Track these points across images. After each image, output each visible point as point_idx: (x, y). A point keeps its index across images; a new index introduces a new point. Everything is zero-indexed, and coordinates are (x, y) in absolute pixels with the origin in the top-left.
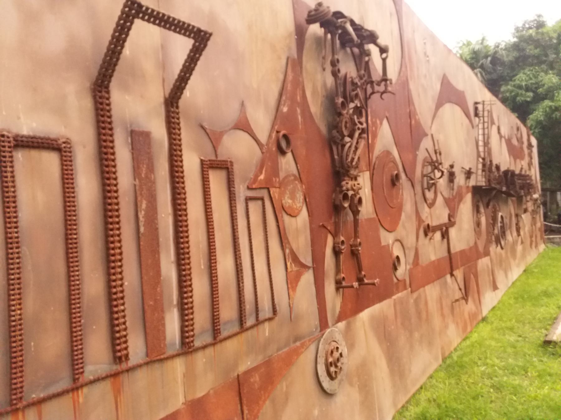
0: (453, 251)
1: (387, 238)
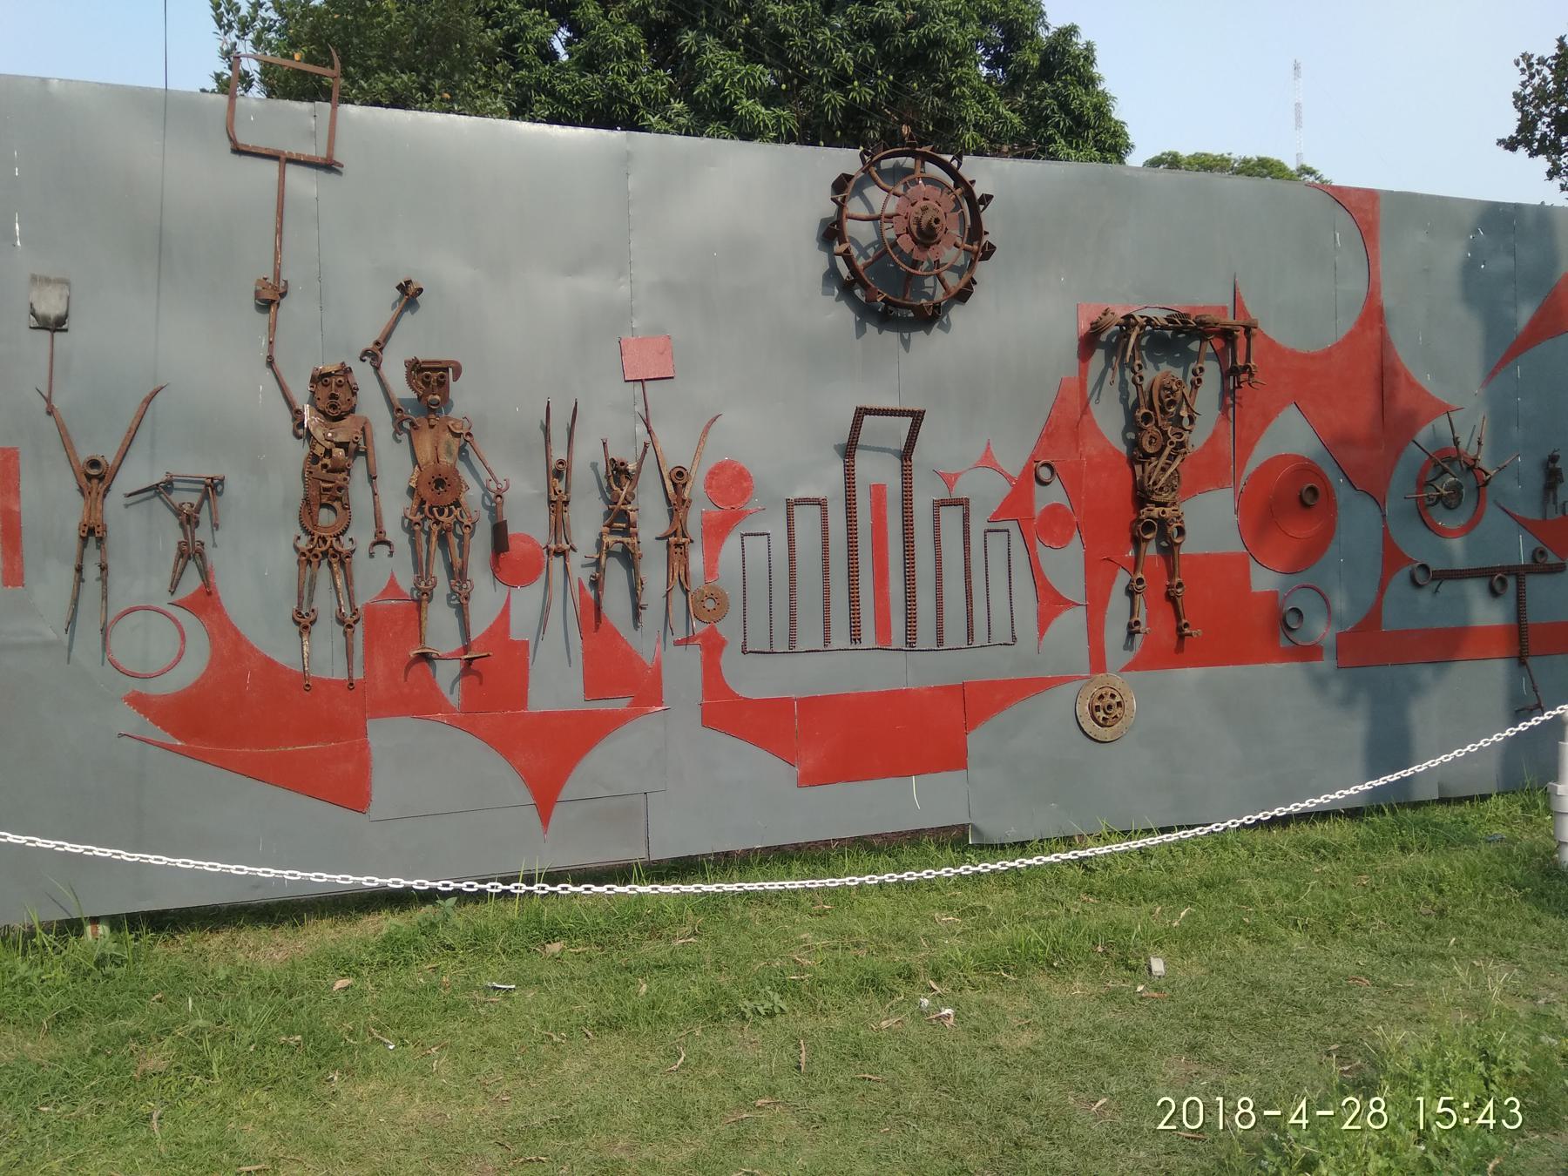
0: (1532, 618)
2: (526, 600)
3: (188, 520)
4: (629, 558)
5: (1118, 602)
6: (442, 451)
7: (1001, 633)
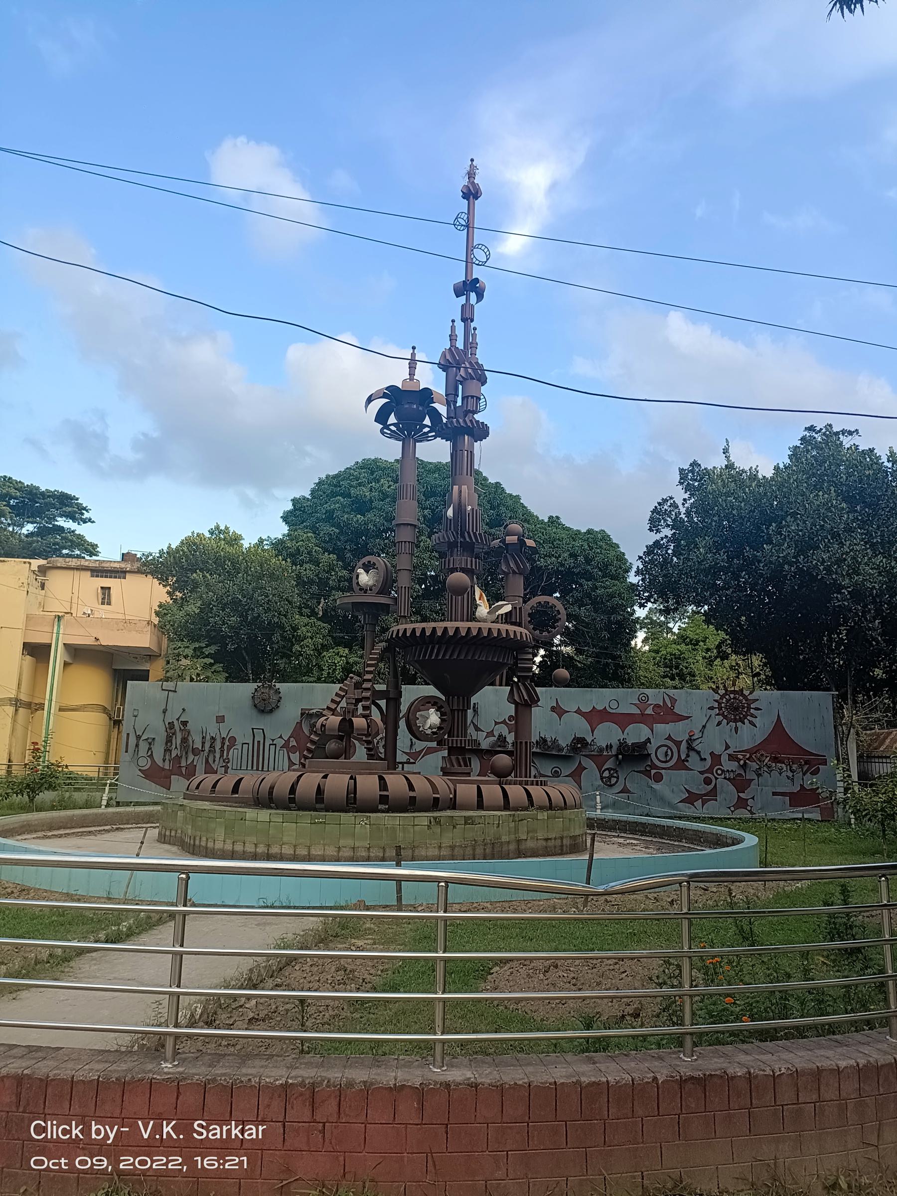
2: (196, 758)
3: (150, 744)
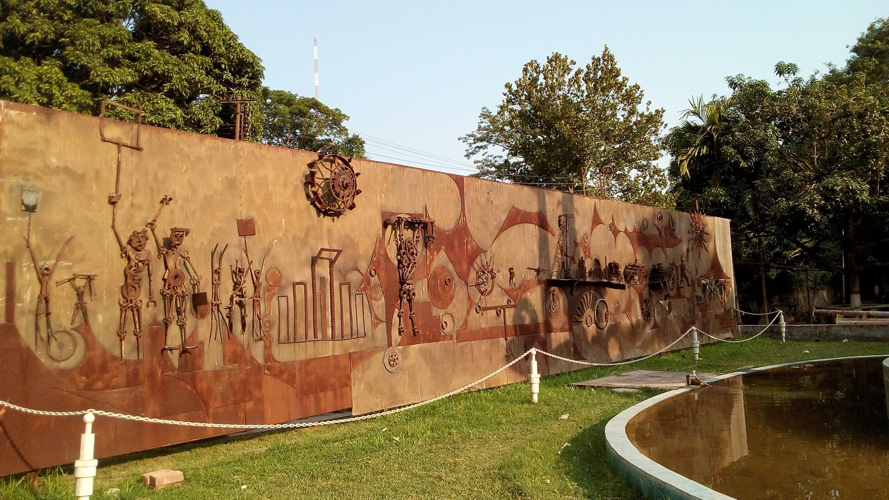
1: (436, 311)
4: (241, 305)
5: (395, 319)
6: (178, 263)
7: (361, 332)
